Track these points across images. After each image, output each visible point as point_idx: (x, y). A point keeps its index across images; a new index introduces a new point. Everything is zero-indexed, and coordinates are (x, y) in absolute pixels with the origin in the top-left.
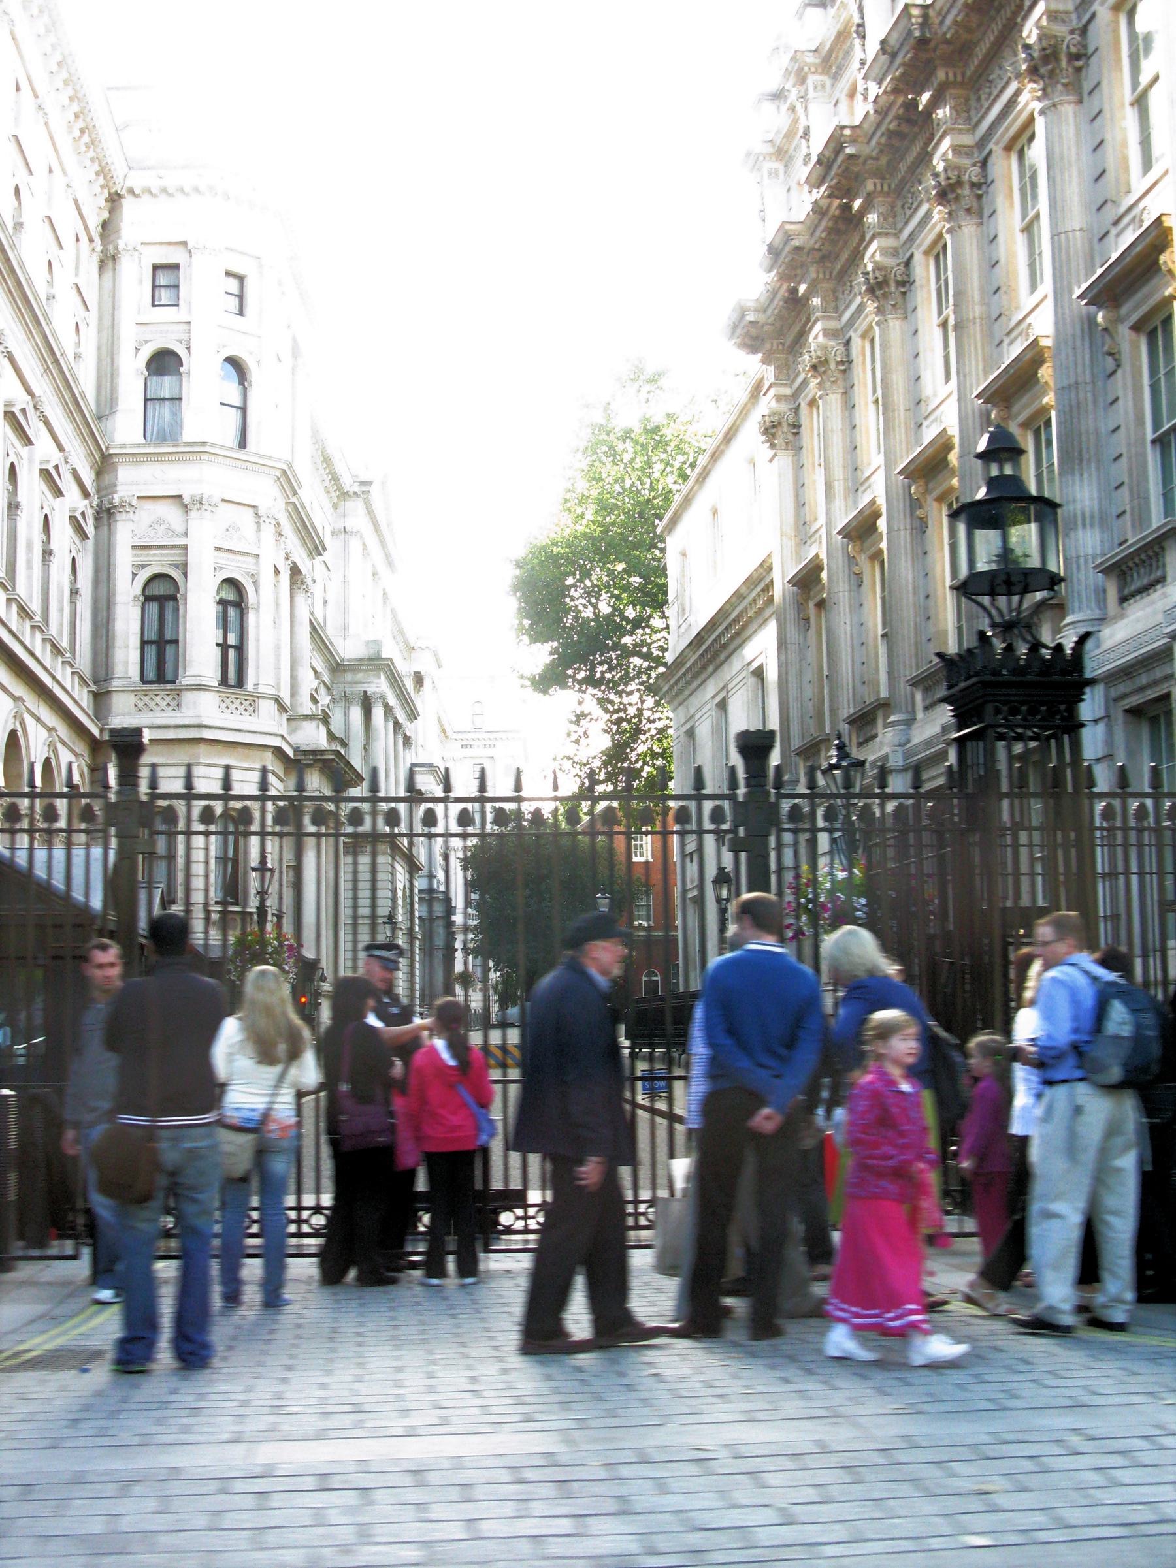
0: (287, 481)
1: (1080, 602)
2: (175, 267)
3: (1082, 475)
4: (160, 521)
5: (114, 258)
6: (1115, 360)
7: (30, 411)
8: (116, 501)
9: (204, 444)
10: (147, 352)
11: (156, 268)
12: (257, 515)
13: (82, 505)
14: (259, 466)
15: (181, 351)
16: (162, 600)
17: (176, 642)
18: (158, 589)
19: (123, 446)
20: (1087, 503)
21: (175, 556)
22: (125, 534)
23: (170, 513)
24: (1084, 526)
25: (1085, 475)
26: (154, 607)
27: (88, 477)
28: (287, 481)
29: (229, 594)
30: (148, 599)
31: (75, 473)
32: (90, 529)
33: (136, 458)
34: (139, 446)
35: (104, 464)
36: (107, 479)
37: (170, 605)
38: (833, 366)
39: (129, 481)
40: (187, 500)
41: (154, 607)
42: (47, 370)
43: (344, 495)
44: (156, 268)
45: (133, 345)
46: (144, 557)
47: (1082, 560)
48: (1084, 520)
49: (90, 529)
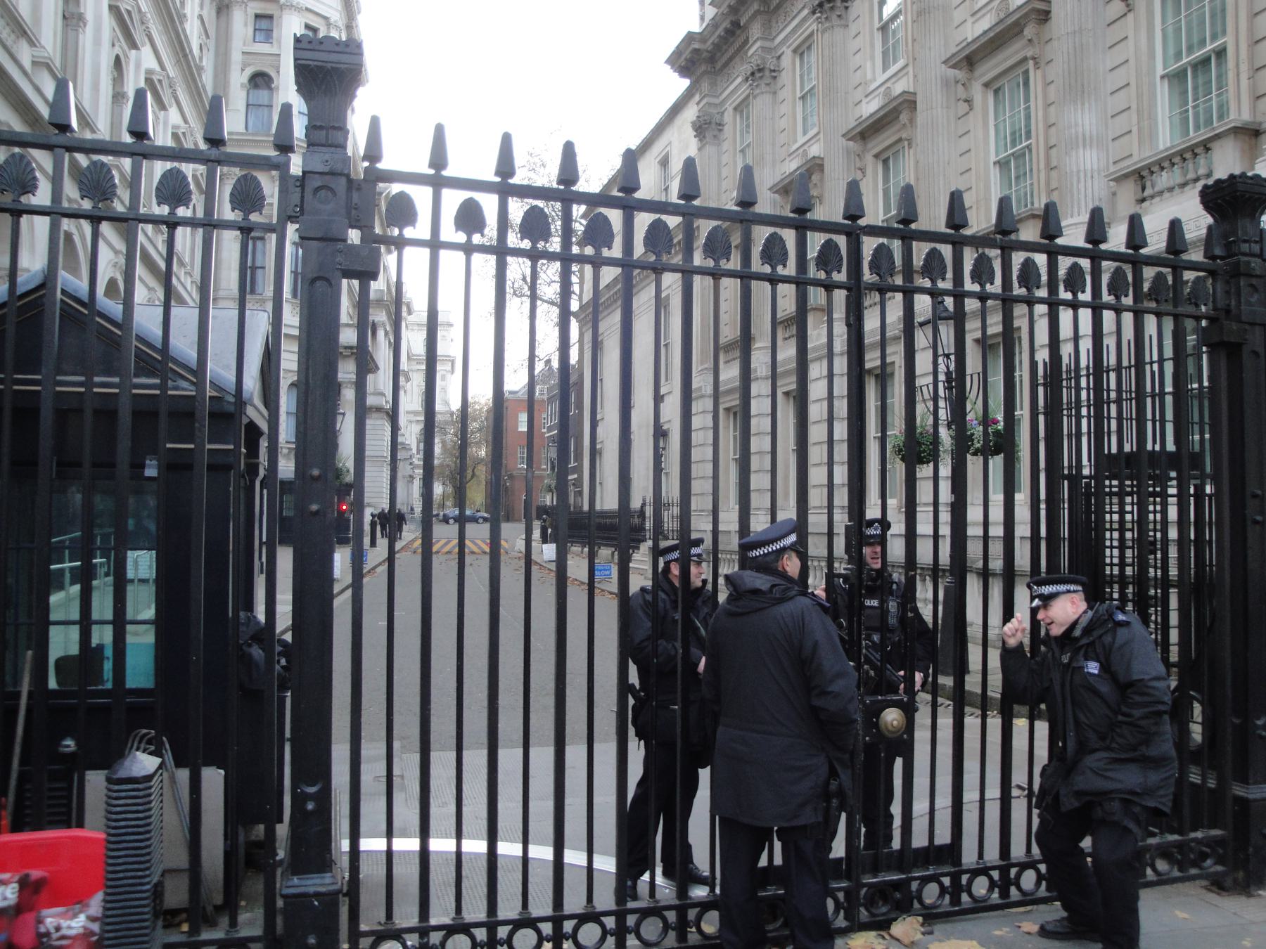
1: (1079, 208)
2: (270, 17)
3: (1083, 104)
5: (228, 7)
6: (1128, 6)
7: (165, 83)
10: (249, 71)
11: (257, 16)
15: (273, 74)
17: (263, 268)
20: (1087, 128)
24: (1084, 147)
25: (1087, 105)
34: (242, 134)
38: (767, 73)
42: (178, 61)
44: (257, 16)
45: (239, 67)
47: (1082, 175)
48: (1084, 140)
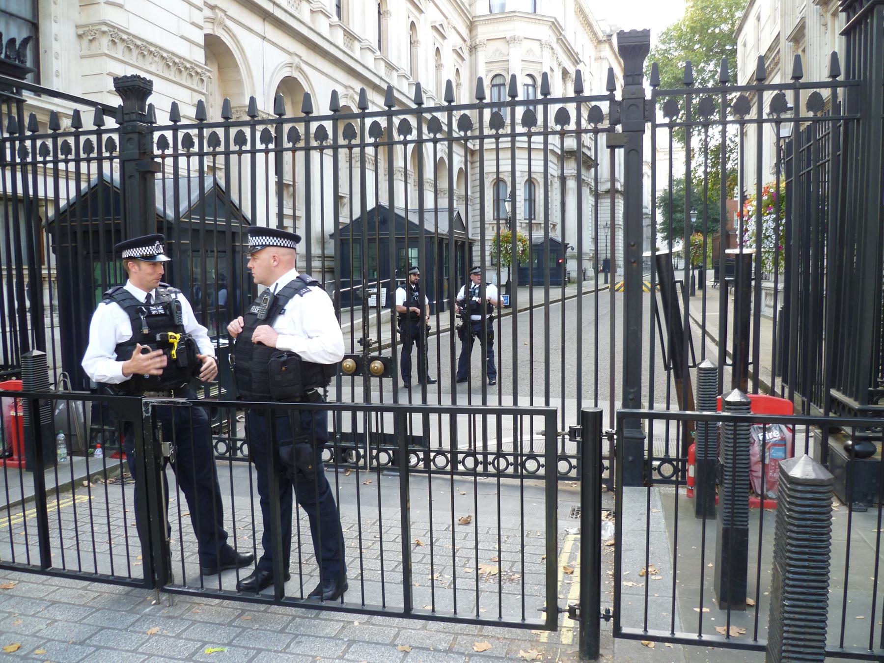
0: (556, 26)
4: (497, 50)
8: (478, 43)
9: (514, 12)
12: (541, 44)
13: (459, 42)
14: (541, 20)
16: (499, 85)
18: (498, 81)
19: (479, 16)
21: (504, 65)
22: (482, 56)
23: (500, 45)
26: (496, 89)
27: (465, 32)
28: (556, 26)
29: (529, 81)
30: (493, 86)
31: (455, 28)
32: (466, 55)
33: (487, 21)
35: (472, 26)
36: (474, 33)
37: (502, 88)
39: (483, 32)
40: (508, 38)
41: (496, 89)
43: (600, 42)
46: (491, 66)
49: (466, 55)
